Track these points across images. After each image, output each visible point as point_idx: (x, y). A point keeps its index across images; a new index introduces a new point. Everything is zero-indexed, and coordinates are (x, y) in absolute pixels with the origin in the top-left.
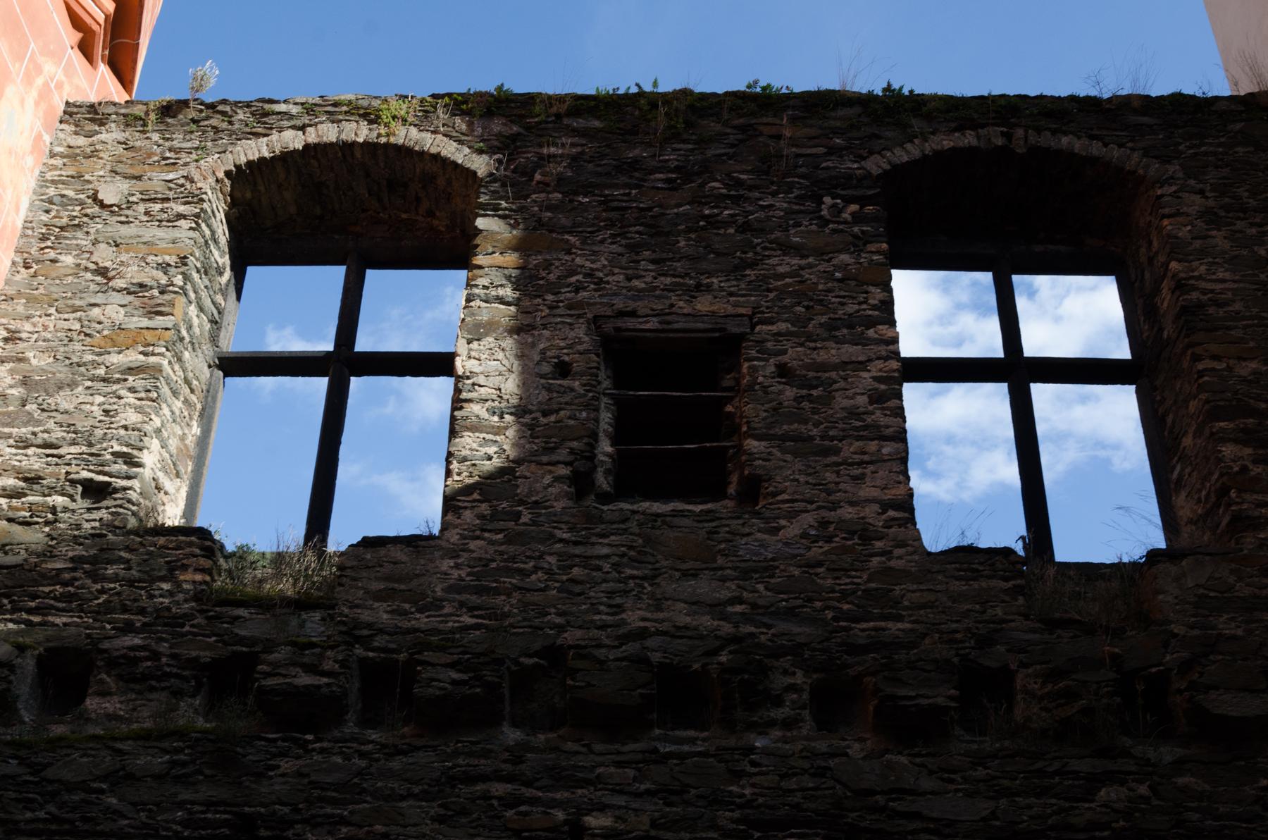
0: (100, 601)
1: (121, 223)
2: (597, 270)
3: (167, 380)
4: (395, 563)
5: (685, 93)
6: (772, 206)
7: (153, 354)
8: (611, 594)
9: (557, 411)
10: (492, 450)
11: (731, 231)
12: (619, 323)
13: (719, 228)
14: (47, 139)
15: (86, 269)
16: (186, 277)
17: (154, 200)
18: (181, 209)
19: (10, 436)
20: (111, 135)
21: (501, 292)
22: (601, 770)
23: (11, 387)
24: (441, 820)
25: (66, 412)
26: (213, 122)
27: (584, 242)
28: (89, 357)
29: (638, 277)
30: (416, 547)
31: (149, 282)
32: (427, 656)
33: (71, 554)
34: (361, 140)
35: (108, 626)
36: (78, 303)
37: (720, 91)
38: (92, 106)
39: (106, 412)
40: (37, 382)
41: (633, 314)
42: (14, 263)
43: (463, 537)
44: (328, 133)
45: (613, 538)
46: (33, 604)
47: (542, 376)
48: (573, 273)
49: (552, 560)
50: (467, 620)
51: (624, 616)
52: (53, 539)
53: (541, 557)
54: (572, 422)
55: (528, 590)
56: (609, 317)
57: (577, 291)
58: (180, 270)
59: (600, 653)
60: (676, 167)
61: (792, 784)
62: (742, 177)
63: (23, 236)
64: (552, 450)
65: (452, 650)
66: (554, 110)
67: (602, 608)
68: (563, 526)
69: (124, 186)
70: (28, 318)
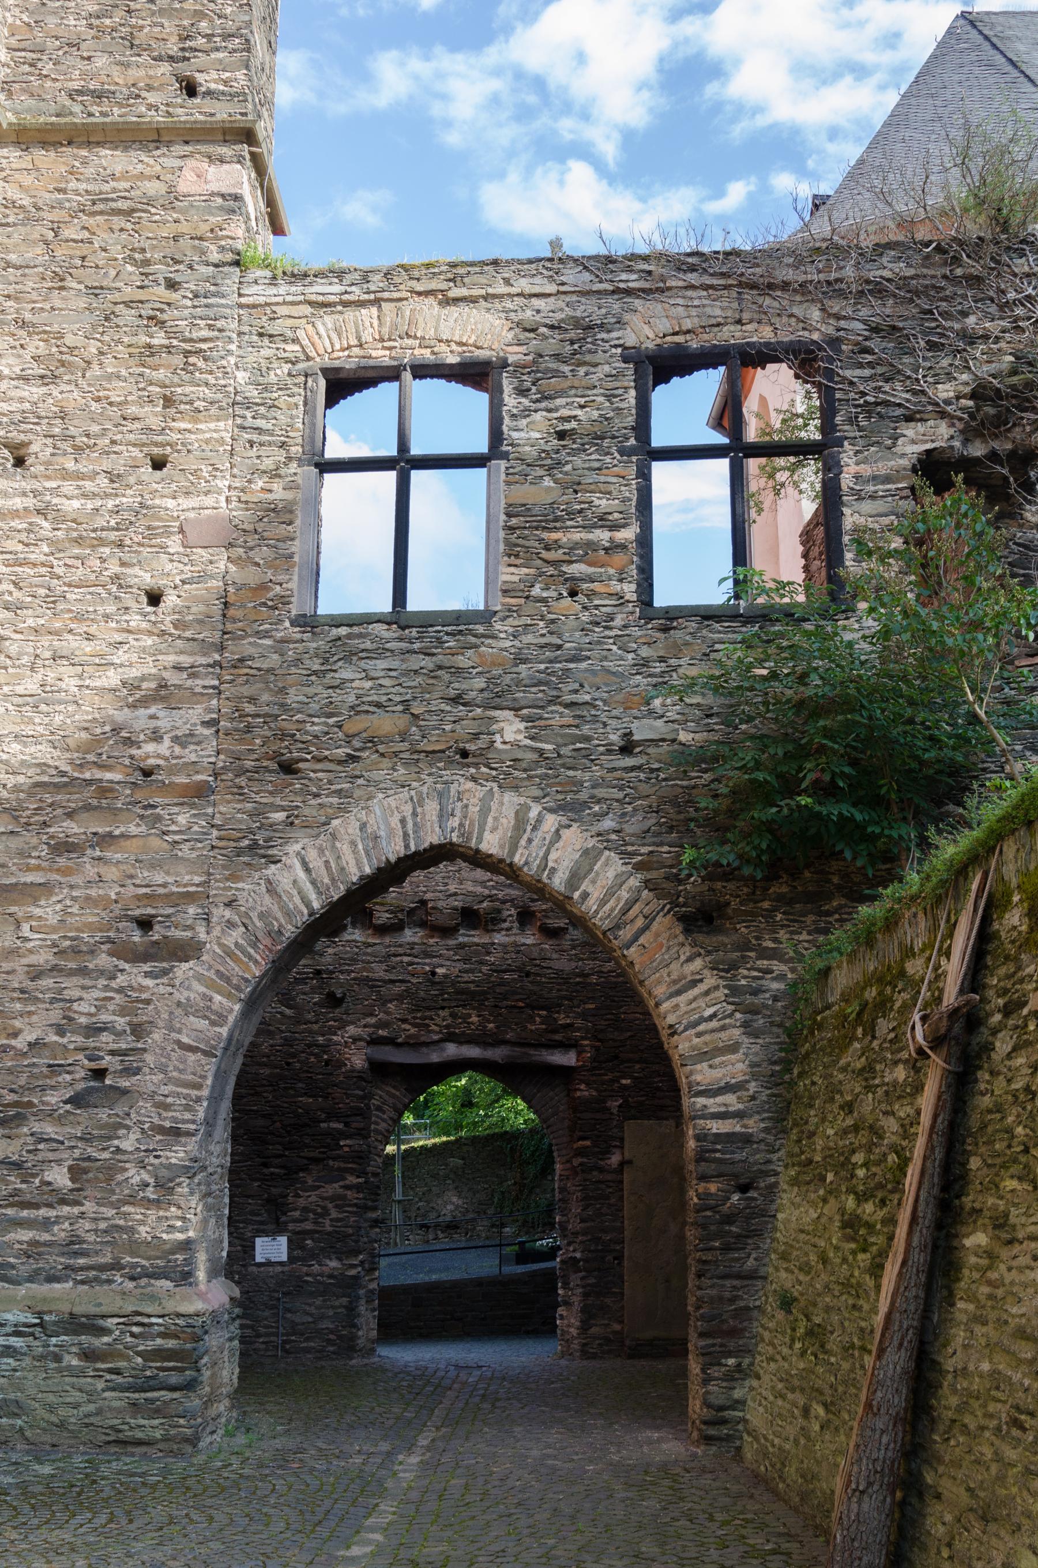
59: (440, 904)
61: (507, 956)
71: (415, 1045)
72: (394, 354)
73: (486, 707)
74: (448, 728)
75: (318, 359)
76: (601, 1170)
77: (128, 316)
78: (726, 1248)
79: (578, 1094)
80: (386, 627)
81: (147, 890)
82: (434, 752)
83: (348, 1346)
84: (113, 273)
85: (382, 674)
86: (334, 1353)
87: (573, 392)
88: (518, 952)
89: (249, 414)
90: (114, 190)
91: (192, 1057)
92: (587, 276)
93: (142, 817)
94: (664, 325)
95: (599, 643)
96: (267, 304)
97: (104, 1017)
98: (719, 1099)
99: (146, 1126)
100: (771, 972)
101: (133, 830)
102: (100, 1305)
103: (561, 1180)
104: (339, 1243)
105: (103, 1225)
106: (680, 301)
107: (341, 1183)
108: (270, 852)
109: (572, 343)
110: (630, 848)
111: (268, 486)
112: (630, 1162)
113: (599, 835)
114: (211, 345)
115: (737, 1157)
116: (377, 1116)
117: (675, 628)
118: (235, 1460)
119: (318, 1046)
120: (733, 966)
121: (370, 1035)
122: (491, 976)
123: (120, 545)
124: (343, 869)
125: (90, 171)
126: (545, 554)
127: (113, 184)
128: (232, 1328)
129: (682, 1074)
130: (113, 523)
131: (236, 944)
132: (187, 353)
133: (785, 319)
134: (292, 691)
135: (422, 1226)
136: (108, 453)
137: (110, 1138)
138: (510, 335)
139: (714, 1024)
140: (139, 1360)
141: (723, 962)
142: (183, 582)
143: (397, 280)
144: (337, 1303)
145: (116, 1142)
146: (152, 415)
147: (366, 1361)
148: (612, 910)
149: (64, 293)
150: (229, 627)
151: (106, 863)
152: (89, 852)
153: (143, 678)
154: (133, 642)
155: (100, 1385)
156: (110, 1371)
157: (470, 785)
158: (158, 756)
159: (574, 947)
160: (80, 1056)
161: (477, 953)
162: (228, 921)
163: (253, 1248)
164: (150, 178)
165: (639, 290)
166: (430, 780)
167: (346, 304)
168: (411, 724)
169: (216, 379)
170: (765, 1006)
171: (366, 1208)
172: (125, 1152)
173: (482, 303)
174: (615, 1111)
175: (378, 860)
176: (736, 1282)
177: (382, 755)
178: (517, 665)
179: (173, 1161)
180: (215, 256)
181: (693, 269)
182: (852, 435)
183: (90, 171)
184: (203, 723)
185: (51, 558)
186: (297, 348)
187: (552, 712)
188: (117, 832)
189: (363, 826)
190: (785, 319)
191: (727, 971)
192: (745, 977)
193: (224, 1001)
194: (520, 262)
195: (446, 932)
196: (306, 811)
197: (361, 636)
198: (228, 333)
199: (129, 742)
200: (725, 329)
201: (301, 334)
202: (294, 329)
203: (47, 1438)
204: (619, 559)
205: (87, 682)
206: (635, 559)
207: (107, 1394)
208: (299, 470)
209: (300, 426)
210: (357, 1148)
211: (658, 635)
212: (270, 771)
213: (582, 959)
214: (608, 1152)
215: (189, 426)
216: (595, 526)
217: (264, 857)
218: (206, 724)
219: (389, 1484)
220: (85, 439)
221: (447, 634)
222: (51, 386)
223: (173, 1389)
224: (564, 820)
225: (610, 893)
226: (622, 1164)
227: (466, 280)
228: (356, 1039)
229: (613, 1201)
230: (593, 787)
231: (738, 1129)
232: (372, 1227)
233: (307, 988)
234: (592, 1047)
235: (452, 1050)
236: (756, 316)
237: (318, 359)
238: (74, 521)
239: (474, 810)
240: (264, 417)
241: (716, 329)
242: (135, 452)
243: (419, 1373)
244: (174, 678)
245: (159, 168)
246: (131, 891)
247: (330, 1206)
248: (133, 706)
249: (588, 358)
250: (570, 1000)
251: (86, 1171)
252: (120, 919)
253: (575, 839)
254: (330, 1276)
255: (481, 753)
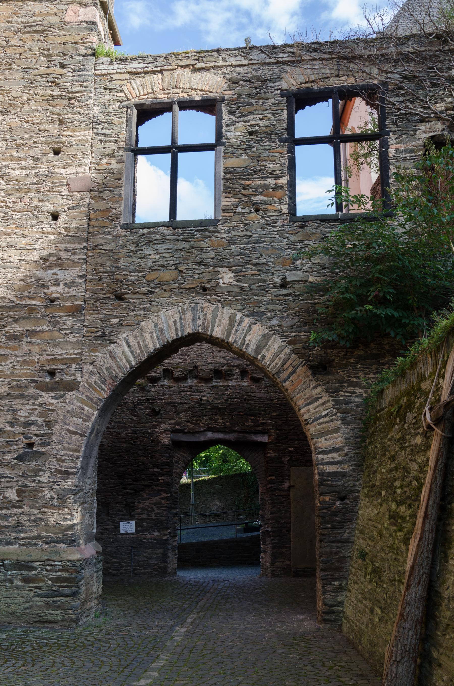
8: (205, 355)
50: (181, 361)
59: (204, 368)
61: (235, 391)
71: (193, 433)
72: (169, 96)
73: (215, 266)
74: (196, 277)
75: (133, 100)
76: (280, 490)
77: (41, 81)
78: (334, 528)
79: (269, 455)
80: (166, 228)
81: (53, 357)
82: (190, 288)
83: (164, 572)
84: (34, 61)
85: (165, 251)
86: (156, 574)
87: (256, 112)
88: (240, 389)
89: (100, 127)
90: (35, 21)
91: (74, 437)
92: (263, 56)
93: (50, 322)
94: (301, 79)
95: (270, 234)
96: (108, 74)
97: (33, 418)
98: (330, 455)
99: (53, 470)
100: (355, 393)
101: (46, 328)
102: (31, 556)
103: (261, 495)
104: (159, 524)
105: (33, 518)
106: (309, 66)
107: (160, 497)
108: (111, 338)
109: (256, 88)
110: (285, 334)
111: (109, 162)
112: (293, 486)
113: (270, 327)
114: (81, 94)
115: (339, 483)
116: (176, 466)
117: (307, 226)
118: (96, 631)
119: (148, 433)
120: (336, 391)
121: (172, 428)
122: (228, 400)
123: (39, 191)
124: (146, 346)
125: (23, 12)
126: (243, 192)
127: (34, 18)
128: (98, 566)
129: (311, 443)
130: (35, 181)
131: (95, 382)
132: (70, 99)
133: (360, 74)
134: (121, 260)
135: (203, 515)
136: (32, 147)
137: (36, 476)
138: (226, 86)
139: (327, 419)
140: (50, 582)
141: (331, 388)
142: (69, 209)
143: (171, 60)
144: (158, 552)
145: (39, 478)
146: (53, 129)
147: (172, 578)
148: (277, 364)
149: (11, 71)
150: (91, 230)
151: (33, 344)
152: (25, 339)
153: (50, 255)
154: (45, 238)
155: (31, 594)
156: (36, 588)
157: (207, 304)
158: (58, 293)
159: (266, 387)
160: (21, 437)
161: (221, 390)
162: (91, 371)
163: (119, 526)
164: (51, 15)
165: (289, 61)
166: (188, 302)
167: (146, 73)
168: (179, 275)
169: (84, 110)
170: (352, 410)
171: (172, 508)
172: (43, 483)
173: (212, 70)
174: (286, 463)
175: (163, 341)
176: (339, 545)
177: (165, 290)
178: (230, 246)
179: (66, 487)
180: (83, 52)
181: (315, 50)
182: (394, 129)
183: (23, 12)
184: (79, 276)
185: (6, 198)
186: (123, 94)
187: (247, 268)
188: (38, 330)
189: (156, 325)
190: (360, 74)
191: (333, 393)
192: (342, 396)
193: (90, 410)
194: (231, 50)
195: (207, 380)
196: (129, 318)
197: (154, 233)
198: (89, 88)
199: (43, 286)
200: (331, 79)
201: (124, 88)
202: (121, 85)
203: (6, 620)
204: (279, 193)
205: (23, 258)
206: (287, 193)
207: (34, 599)
208: (124, 154)
209: (125, 132)
210: (166, 480)
211: (299, 229)
212: (111, 299)
213: (270, 393)
214: (283, 482)
215: (71, 134)
216: (267, 177)
217: (108, 340)
218: (80, 277)
219: (168, 643)
220: (21, 141)
221: (196, 231)
222: (5, 116)
223: (66, 596)
224: (253, 321)
225: (276, 356)
226: (290, 487)
227: (204, 59)
228: (165, 430)
229: (285, 504)
230: (267, 304)
231: (339, 470)
232: (174, 517)
233: (143, 407)
234: (275, 433)
235: (210, 435)
236: (346, 73)
237: (133, 100)
238: (16, 180)
239: (209, 316)
240: (107, 128)
241: (327, 80)
242: (46, 147)
243: (195, 584)
244: (64, 255)
245: (56, 10)
246: (45, 357)
247: (154, 507)
248: (45, 269)
249: (264, 95)
250: (265, 411)
251: (24, 492)
252: (40, 371)
253: (258, 330)
254: (155, 539)
255: (212, 289)
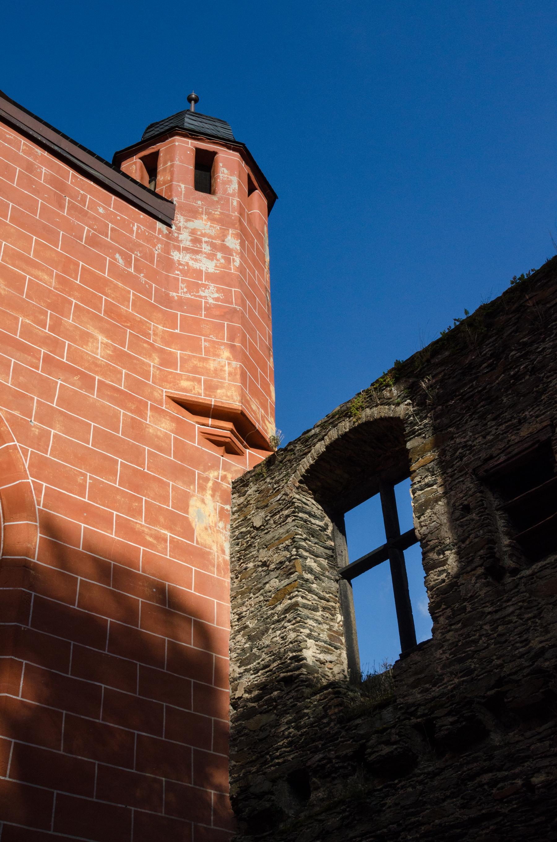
0: (302, 740)
1: (266, 533)
2: (468, 441)
3: (305, 606)
4: (416, 664)
5: (483, 308)
6: (544, 348)
7: (293, 597)
8: (520, 634)
9: (468, 537)
10: (443, 576)
11: (527, 377)
12: (486, 467)
13: (521, 379)
14: (228, 507)
15: (259, 566)
16: (297, 548)
17: (275, 514)
18: (286, 512)
19: (250, 669)
20: (251, 490)
21: (426, 480)
22: (532, 747)
23: (245, 643)
24: (463, 806)
25: (268, 646)
26: (288, 458)
27: (458, 428)
28: (270, 612)
29: (488, 434)
30: (423, 650)
31: (283, 559)
32: (437, 713)
33: (285, 720)
34: (348, 430)
35: (309, 752)
36: (259, 586)
37: (500, 295)
38: (241, 479)
39: (282, 638)
40: (254, 636)
41: (491, 457)
42: (232, 579)
43: (443, 634)
44: (334, 434)
45: (513, 599)
46: (278, 754)
47: (457, 520)
48: (456, 450)
49: (487, 627)
50: (456, 681)
51: (531, 645)
52: (278, 716)
53: (481, 628)
54: (477, 540)
55: (480, 651)
56: (480, 466)
57: (461, 460)
58: (293, 546)
60: (491, 355)
62: (525, 340)
63: (232, 562)
64: (470, 562)
65: (446, 705)
66: (424, 359)
67: (518, 645)
68: (487, 604)
69: (262, 514)
70: (243, 604)
